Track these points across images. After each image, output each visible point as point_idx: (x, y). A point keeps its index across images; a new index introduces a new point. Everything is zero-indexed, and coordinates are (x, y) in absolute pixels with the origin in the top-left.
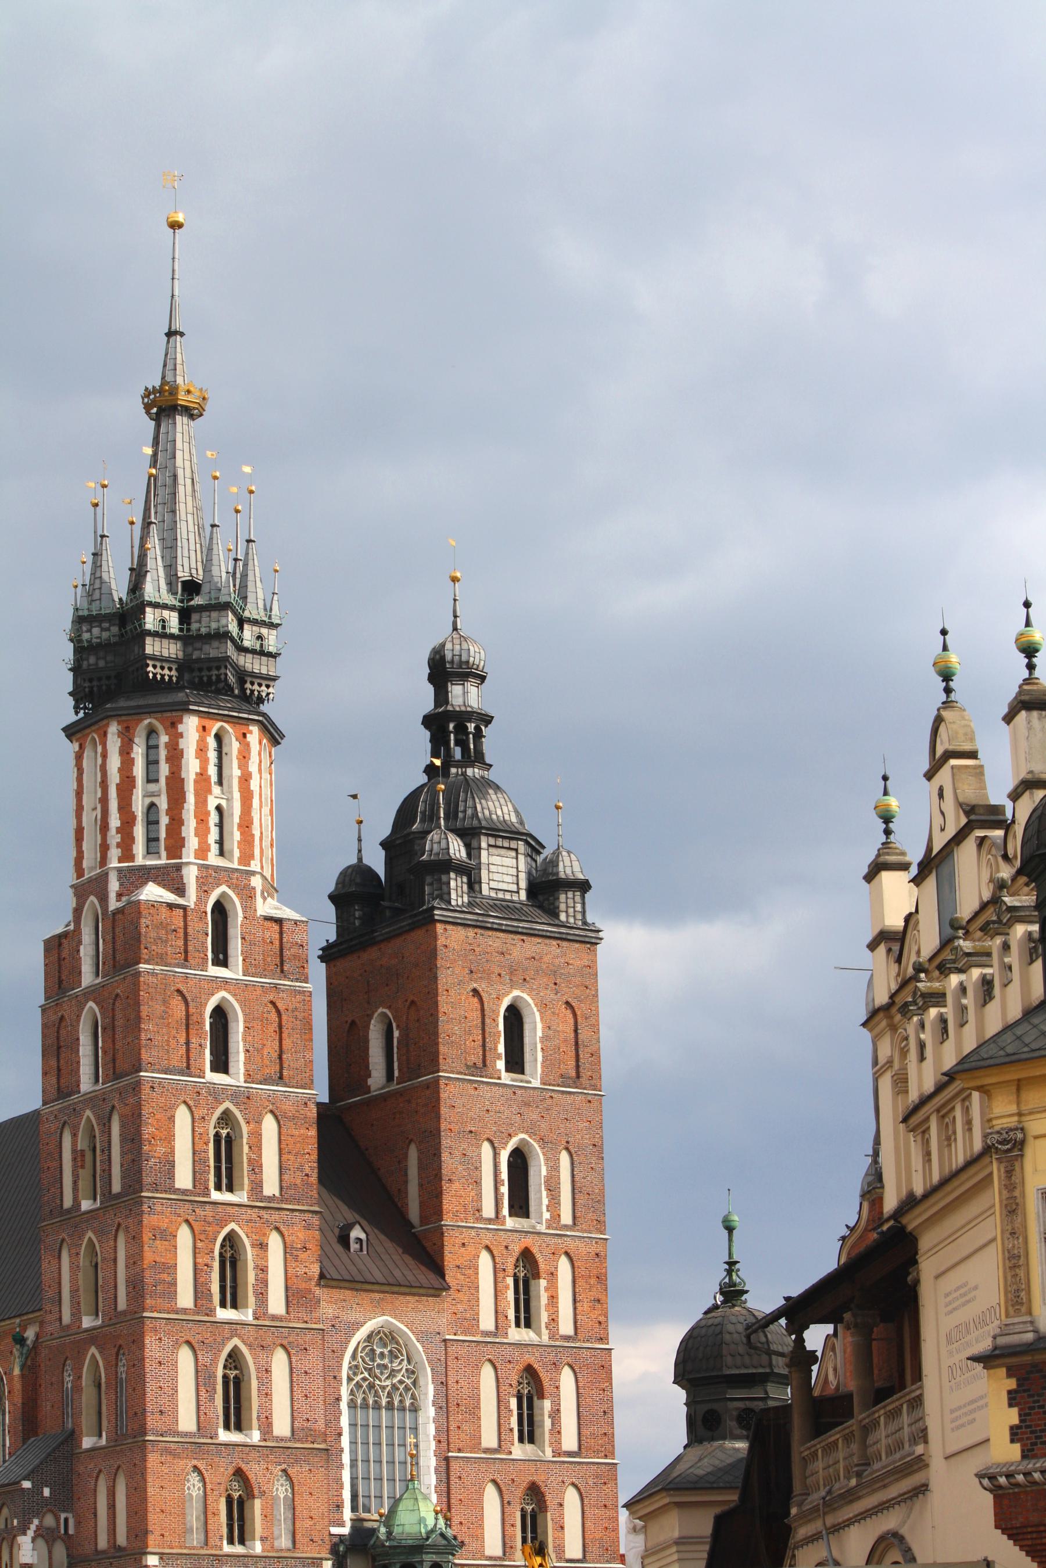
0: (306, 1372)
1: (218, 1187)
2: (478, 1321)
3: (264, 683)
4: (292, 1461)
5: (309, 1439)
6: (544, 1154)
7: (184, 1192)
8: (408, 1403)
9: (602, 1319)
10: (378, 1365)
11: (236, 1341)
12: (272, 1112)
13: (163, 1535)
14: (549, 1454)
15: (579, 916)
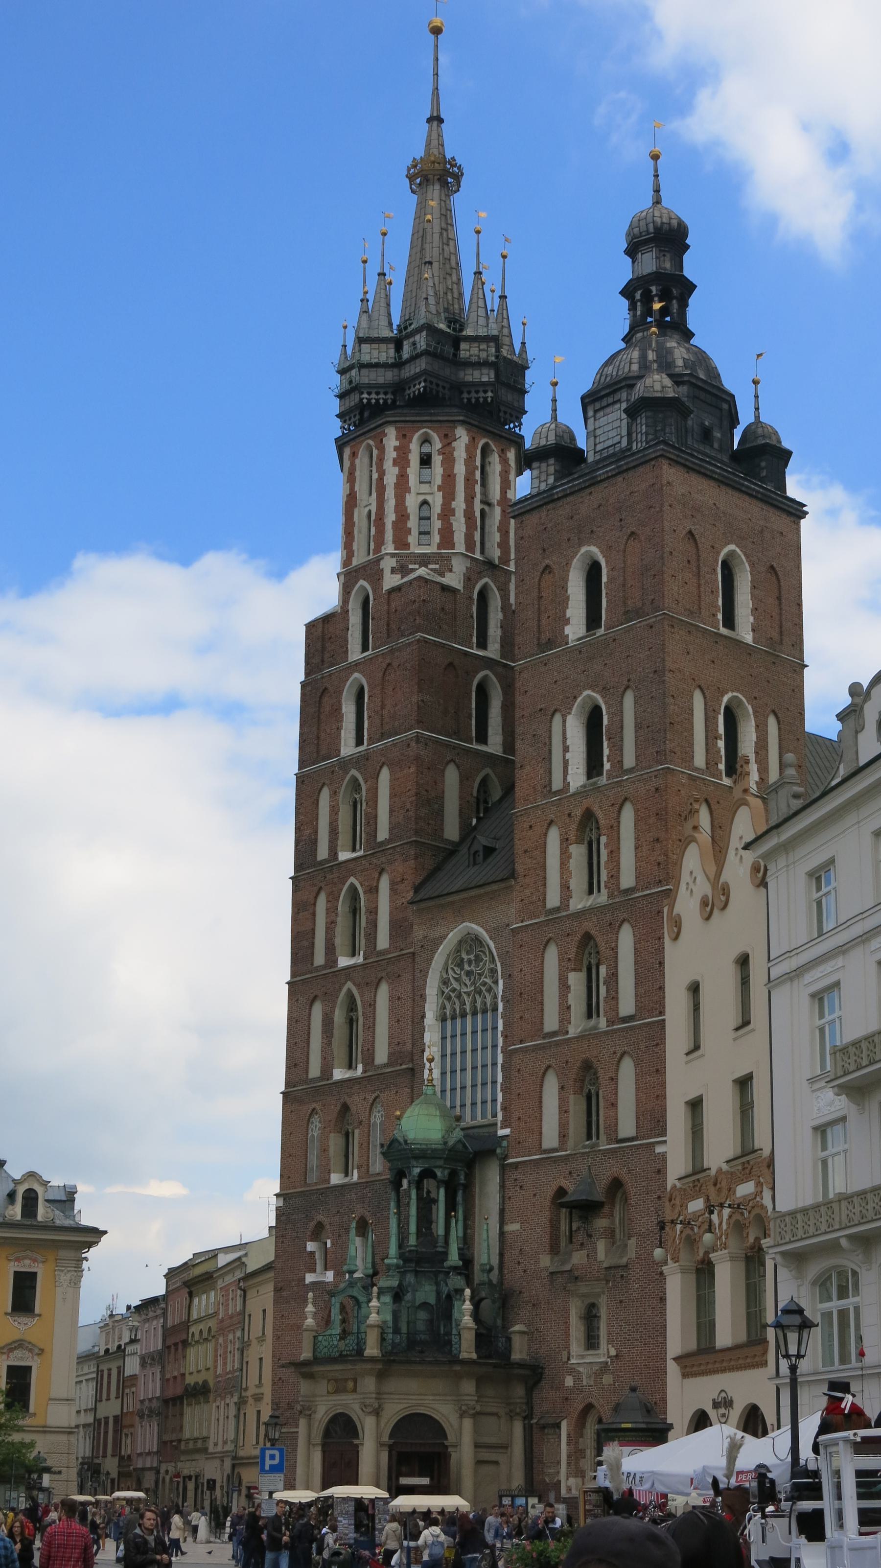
0: (399, 998)
1: (354, 850)
2: (544, 899)
3: (417, 382)
4: (384, 1086)
5: (399, 1061)
6: (606, 703)
7: (322, 863)
8: (489, 1001)
9: (661, 859)
10: (469, 974)
11: (349, 985)
12: (383, 764)
13: (289, 1177)
14: (603, 1023)
15: (644, 439)
